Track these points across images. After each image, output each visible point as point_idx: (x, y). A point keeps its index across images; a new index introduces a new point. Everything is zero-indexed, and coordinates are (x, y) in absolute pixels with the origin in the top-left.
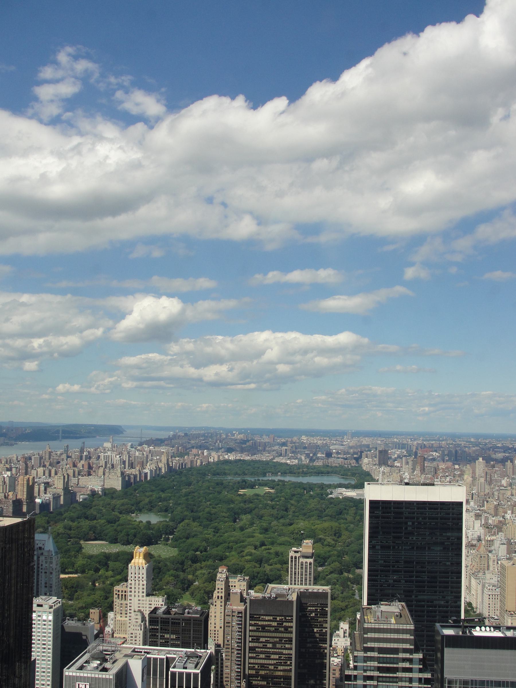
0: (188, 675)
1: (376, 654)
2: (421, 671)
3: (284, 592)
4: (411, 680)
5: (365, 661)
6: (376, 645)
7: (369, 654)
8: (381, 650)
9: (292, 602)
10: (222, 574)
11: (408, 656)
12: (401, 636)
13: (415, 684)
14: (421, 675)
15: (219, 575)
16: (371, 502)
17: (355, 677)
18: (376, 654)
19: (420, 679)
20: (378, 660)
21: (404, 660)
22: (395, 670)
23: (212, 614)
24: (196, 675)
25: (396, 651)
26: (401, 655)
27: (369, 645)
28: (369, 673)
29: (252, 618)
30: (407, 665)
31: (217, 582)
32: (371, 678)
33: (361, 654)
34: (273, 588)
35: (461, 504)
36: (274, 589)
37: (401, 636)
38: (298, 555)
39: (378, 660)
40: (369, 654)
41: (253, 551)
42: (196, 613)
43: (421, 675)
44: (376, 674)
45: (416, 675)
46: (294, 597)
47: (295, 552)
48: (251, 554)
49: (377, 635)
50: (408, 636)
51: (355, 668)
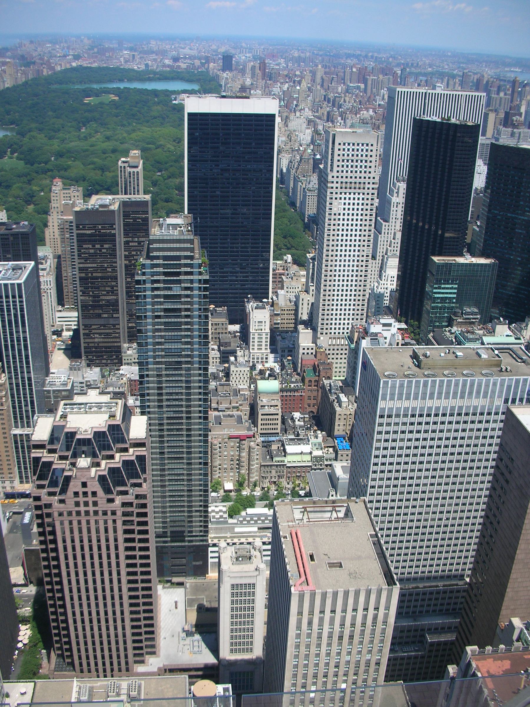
0: (13, 285)
1: (161, 262)
2: (200, 273)
3: (107, 202)
4: (192, 282)
5: (152, 268)
6: (161, 254)
7: (155, 262)
8: (165, 258)
9: (113, 211)
10: (58, 185)
11: (189, 261)
12: (182, 245)
13: (196, 285)
14: (200, 277)
15: (54, 188)
16: (190, 114)
17: (144, 281)
18: (161, 262)
19: (200, 280)
20: (164, 266)
21: (186, 265)
22: (179, 274)
23: (50, 224)
24: (19, 285)
25: (178, 258)
26: (183, 262)
27: (155, 254)
28: (155, 278)
29: (78, 228)
30: (189, 270)
31: (52, 194)
32: (158, 281)
33: (148, 262)
34: (98, 199)
35: (273, 116)
36: (96, 201)
37: (182, 245)
38: (126, 165)
39: (164, 266)
40: (155, 262)
41: (96, 160)
42: (23, 228)
43: (200, 277)
44: (162, 278)
45: (196, 277)
46: (115, 207)
47: (124, 162)
48: (93, 163)
49: (161, 246)
50: (189, 245)
51: (144, 274)
